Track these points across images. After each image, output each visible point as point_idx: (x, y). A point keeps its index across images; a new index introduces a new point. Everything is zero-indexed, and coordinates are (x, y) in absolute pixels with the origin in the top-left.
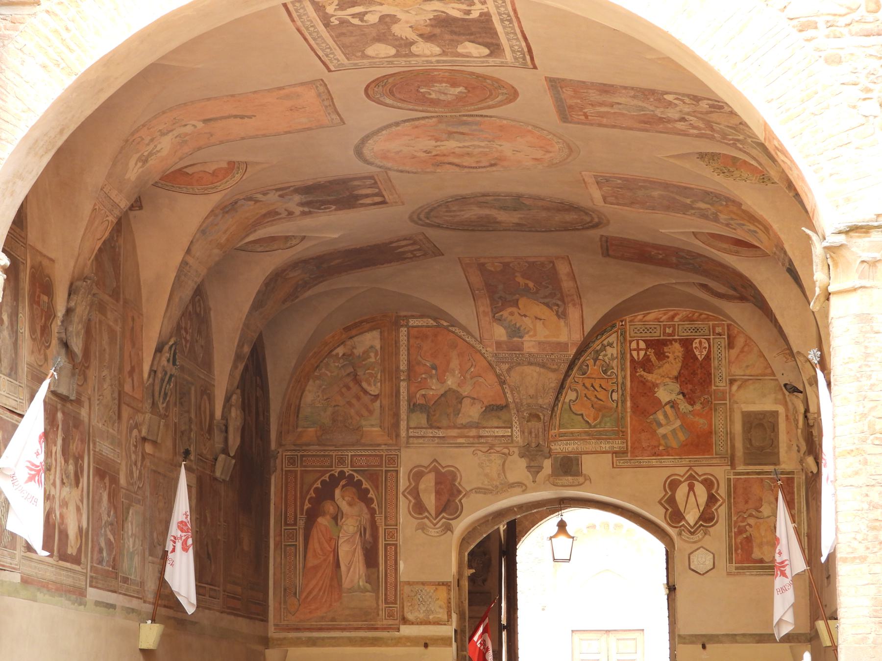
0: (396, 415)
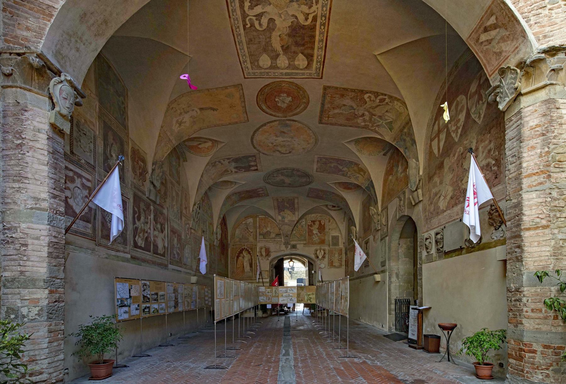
0: (256, 236)
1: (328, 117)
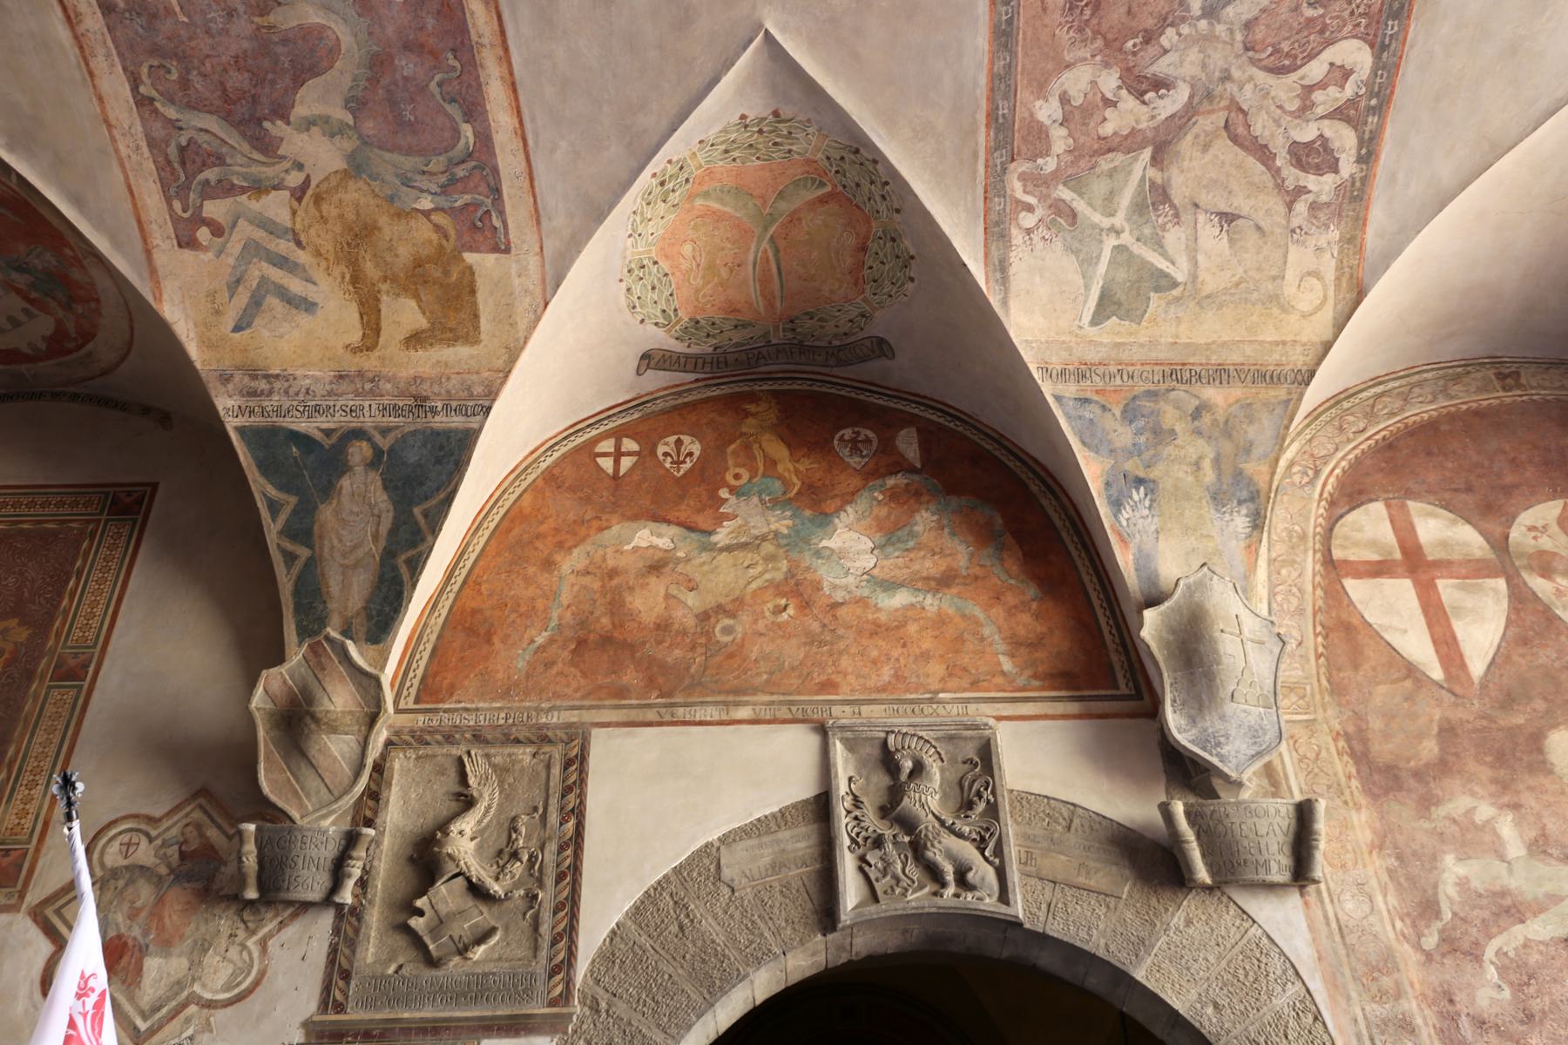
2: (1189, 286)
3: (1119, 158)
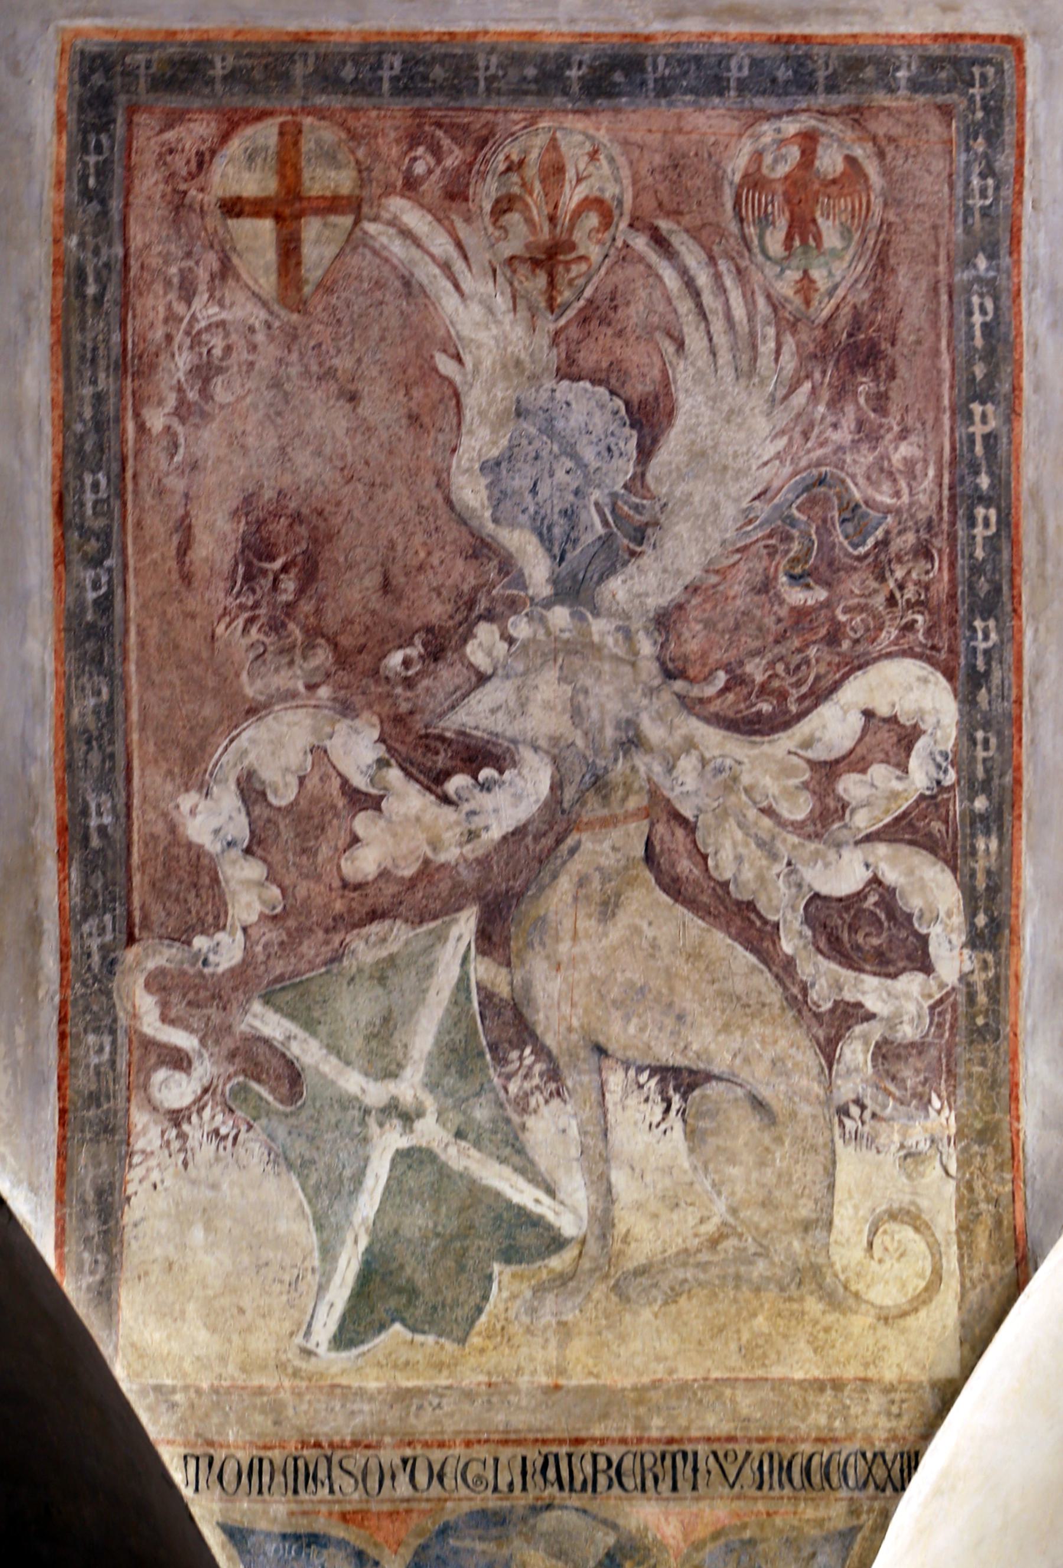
1: (287, 208)
2: (593, 1247)
3: (398, 936)
